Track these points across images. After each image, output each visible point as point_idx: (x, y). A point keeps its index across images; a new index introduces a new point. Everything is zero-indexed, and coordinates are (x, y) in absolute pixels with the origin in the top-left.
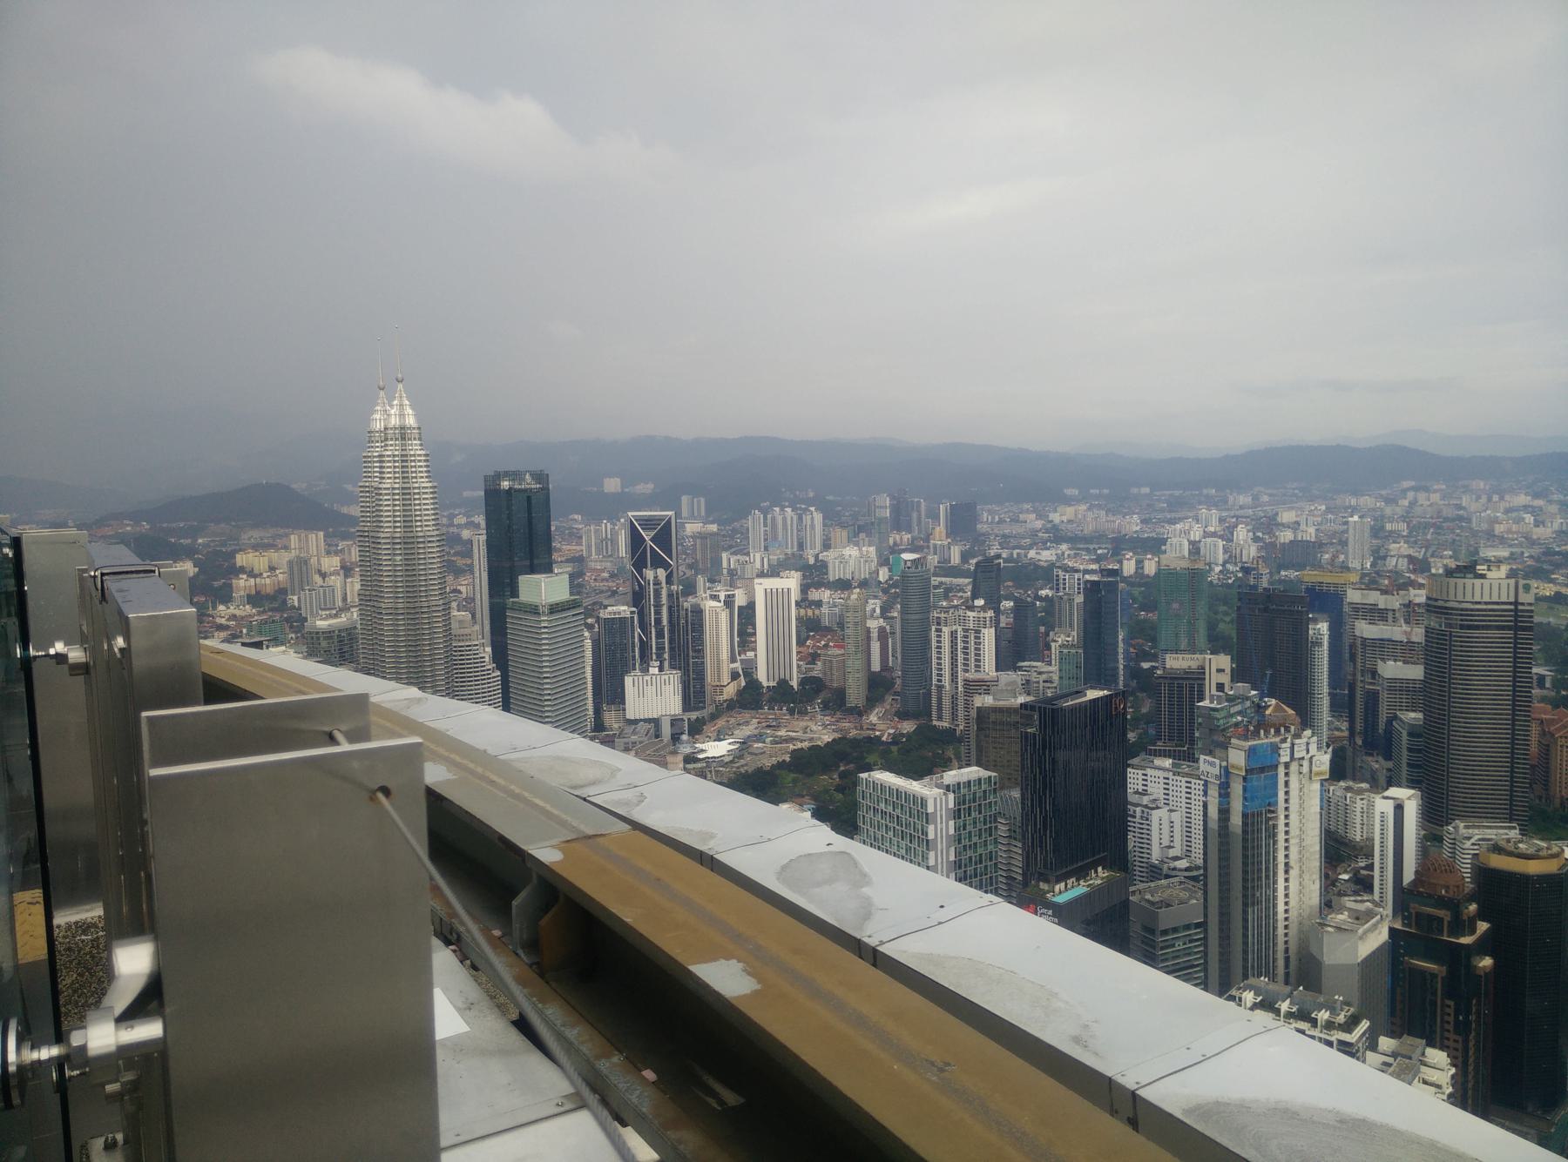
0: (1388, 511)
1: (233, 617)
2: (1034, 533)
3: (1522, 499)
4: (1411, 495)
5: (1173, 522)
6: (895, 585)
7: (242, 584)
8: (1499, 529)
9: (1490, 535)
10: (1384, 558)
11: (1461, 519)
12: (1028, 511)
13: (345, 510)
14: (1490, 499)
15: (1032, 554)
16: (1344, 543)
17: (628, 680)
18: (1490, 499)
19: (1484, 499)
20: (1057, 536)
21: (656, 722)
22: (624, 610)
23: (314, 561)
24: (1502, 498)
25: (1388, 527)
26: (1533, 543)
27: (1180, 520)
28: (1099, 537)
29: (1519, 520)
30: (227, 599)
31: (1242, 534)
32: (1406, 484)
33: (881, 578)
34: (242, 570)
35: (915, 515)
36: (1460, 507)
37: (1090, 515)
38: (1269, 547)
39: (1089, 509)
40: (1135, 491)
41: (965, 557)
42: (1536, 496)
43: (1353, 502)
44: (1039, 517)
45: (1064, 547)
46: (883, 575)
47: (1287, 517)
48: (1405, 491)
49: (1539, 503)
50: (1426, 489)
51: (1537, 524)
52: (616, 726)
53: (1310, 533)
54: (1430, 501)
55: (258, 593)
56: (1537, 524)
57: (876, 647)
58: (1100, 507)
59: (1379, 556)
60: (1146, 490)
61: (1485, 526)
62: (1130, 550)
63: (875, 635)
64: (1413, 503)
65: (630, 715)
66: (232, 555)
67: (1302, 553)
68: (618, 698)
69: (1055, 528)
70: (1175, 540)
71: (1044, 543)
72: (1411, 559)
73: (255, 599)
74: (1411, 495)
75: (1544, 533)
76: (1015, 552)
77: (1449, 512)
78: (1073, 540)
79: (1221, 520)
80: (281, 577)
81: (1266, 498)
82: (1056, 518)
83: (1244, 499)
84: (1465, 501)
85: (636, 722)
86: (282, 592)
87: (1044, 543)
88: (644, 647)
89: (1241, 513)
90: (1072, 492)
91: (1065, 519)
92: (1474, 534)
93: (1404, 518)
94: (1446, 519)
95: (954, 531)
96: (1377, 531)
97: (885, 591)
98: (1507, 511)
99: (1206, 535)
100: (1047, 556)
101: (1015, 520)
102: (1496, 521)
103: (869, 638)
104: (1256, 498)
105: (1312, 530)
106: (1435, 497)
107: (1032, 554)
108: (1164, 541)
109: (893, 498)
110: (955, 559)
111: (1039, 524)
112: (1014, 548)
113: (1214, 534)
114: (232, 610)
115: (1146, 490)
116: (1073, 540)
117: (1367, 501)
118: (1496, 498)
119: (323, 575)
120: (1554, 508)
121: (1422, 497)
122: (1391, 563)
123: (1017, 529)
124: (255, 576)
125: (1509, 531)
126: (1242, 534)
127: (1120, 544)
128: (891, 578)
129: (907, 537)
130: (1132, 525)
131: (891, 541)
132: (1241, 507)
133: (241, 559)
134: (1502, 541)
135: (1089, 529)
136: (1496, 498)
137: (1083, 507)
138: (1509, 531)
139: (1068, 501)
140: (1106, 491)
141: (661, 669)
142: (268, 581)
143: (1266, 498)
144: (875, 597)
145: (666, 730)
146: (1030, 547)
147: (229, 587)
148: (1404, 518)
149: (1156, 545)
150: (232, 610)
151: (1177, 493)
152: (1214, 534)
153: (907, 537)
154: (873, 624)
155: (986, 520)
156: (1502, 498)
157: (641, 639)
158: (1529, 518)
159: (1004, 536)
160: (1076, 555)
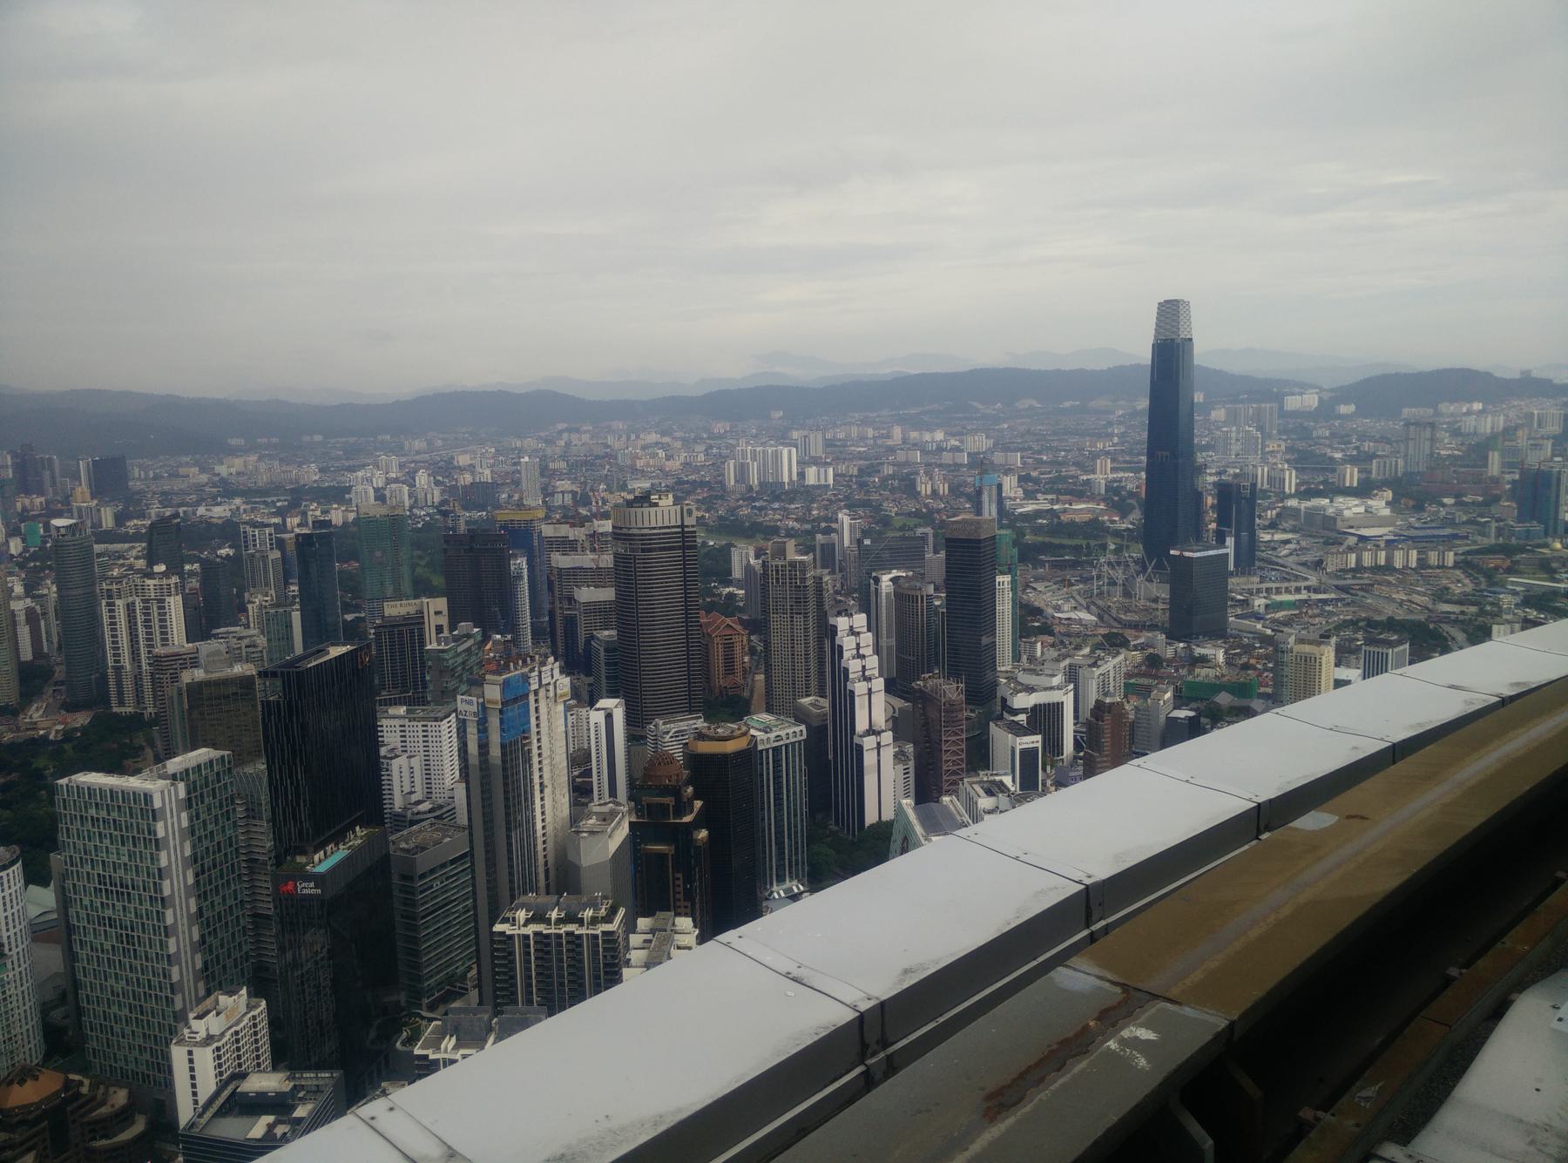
0: (549, 451)
2: (199, 488)
3: (653, 437)
4: (565, 435)
5: (352, 469)
6: (34, 557)
8: (640, 464)
9: (634, 470)
10: (552, 494)
11: (607, 455)
12: (187, 465)
14: (628, 438)
15: (201, 511)
16: (517, 483)
18: (628, 438)
19: (624, 438)
20: (227, 490)
24: (638, 437)
25: (551, 465)
26: (667, 475)
27: (363, 466)
28: (274, 489)
29: (654, 456)
31: (422, 479)
32: (561, 426)
33: (13, 551)
35: (47, 474)
36: (608, 446)
37: (262, 466)
38: (452, 490)
39: (260, 459)
40: (306, 438)
41: (120, 519)
42: (663, 434)
43: (519, 444)
44: (203, 470)
45: (238, 501)
46: (15, 547)
47: (463, 460)
48: (561, 432)
49: (666, 440)
50: (578, 431)
51: (668, 458)
53: (486, 475)
54: (582, 441)
56: (668, 458)
57: (24, 632)
58: (271, 457)
59: (547, 492)
60: (318, 438)
61: (629, 462)
62: (313, 500)
63: (22, 618)
64: (568, 444)
67: (480, 495)
69: (223, 481)
70: (360, 488)
71: (214, 498)
72: (574, 493)
74: (565, 435)
75: (674, 465)
76: (181, 510)
77: (600, 451)
78: (247, 493)
79: (402, 466)
81: (440, 443)
82: (223, 470)
83: (419, 444)
84: (610, 440)
87: (214, 498)
89: (418, 458)
90: (234, 442)
91: (233, 470)
92: (621, 469)
93: (563, 457)
94: (597, 457)
95: (98, 491)
96: (544, 471)
97: (22, 566)
98: (644, 448)
99: (389, 481)
100: (220, 512)
101: (174, 475)
102: (637, 457)
103: (14, 624)
104: (430, 443)
105: (487, 472)
106: (586, 437)
107: (201, 511)
108: (348, 489)
109: (14, 455)
110: (108, 521)
111: (204, 478)
112: (179, 505)
113: (396, 480)
115: (318, 438)
116: (247, 493)
117: (530, 443)
118: (633, 437)
120: (678, 444)
121: (574, 436)
122: (558, 500)
123: (178, 485)
125: (648, 465)
126: (422, 479)
127: (298, 497)
128: (25, 550)
129: (39, 500)
130: (311, 474)
131: (19, 505)
132: (418, 453)
134: (643, 474)
135: (263, 480)
136: (633, 437)
137: (253, 458)
138: (648, 465)
139: (234, 452)
140: (274, 440)
143: (440, 443)
144: (11, 574)
146: (198, 503)
148: (563, 457)
149: (339, 494)
151: (352, 440)
152: (396, 480)
153: (39, 500)
154: (18, 606)
155: (137, 476)
156: (638, 437)
158: (661, 453)
159: (164, 493)
160: (253, 510)
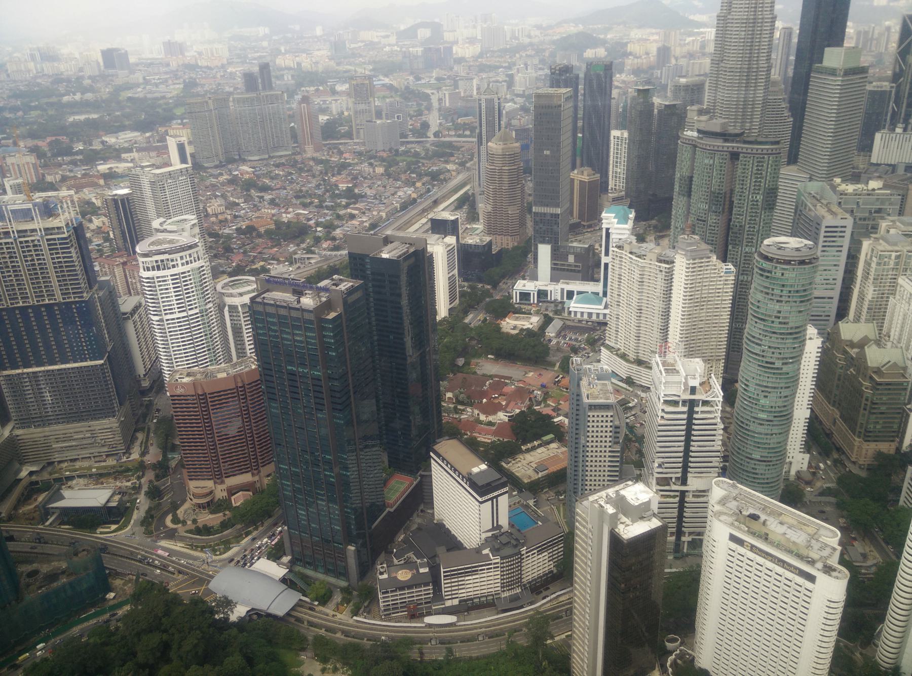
1: (624, 82)
7: (630, 62)
13: (691, 17)
17: (878, 136)
21: (893, 167)
22: (886, 85)
23: (672, 48)
30: (621, 72)
34: (631, 54)
52: (862, 166)
55: (638, 68)
65: (874, 160)
66: (626, 44)
68: (866, 147)
73: (636, 72)
80: (652, 59)
85: (878, 165)
86: (651, 68)
88: (894, 114)
114: (623, 77)
119: (676, 59)
124: (637, 58)
133: (630, 48)
141: (905, 130)
142: (645, 61)
145: (901, 171)
147: (623, 64)
150: (623, 77)
157: (893, 108)
